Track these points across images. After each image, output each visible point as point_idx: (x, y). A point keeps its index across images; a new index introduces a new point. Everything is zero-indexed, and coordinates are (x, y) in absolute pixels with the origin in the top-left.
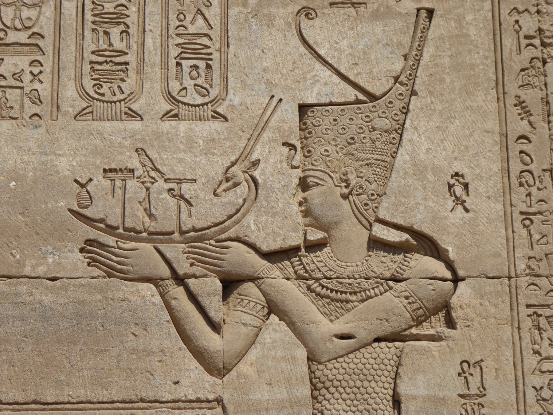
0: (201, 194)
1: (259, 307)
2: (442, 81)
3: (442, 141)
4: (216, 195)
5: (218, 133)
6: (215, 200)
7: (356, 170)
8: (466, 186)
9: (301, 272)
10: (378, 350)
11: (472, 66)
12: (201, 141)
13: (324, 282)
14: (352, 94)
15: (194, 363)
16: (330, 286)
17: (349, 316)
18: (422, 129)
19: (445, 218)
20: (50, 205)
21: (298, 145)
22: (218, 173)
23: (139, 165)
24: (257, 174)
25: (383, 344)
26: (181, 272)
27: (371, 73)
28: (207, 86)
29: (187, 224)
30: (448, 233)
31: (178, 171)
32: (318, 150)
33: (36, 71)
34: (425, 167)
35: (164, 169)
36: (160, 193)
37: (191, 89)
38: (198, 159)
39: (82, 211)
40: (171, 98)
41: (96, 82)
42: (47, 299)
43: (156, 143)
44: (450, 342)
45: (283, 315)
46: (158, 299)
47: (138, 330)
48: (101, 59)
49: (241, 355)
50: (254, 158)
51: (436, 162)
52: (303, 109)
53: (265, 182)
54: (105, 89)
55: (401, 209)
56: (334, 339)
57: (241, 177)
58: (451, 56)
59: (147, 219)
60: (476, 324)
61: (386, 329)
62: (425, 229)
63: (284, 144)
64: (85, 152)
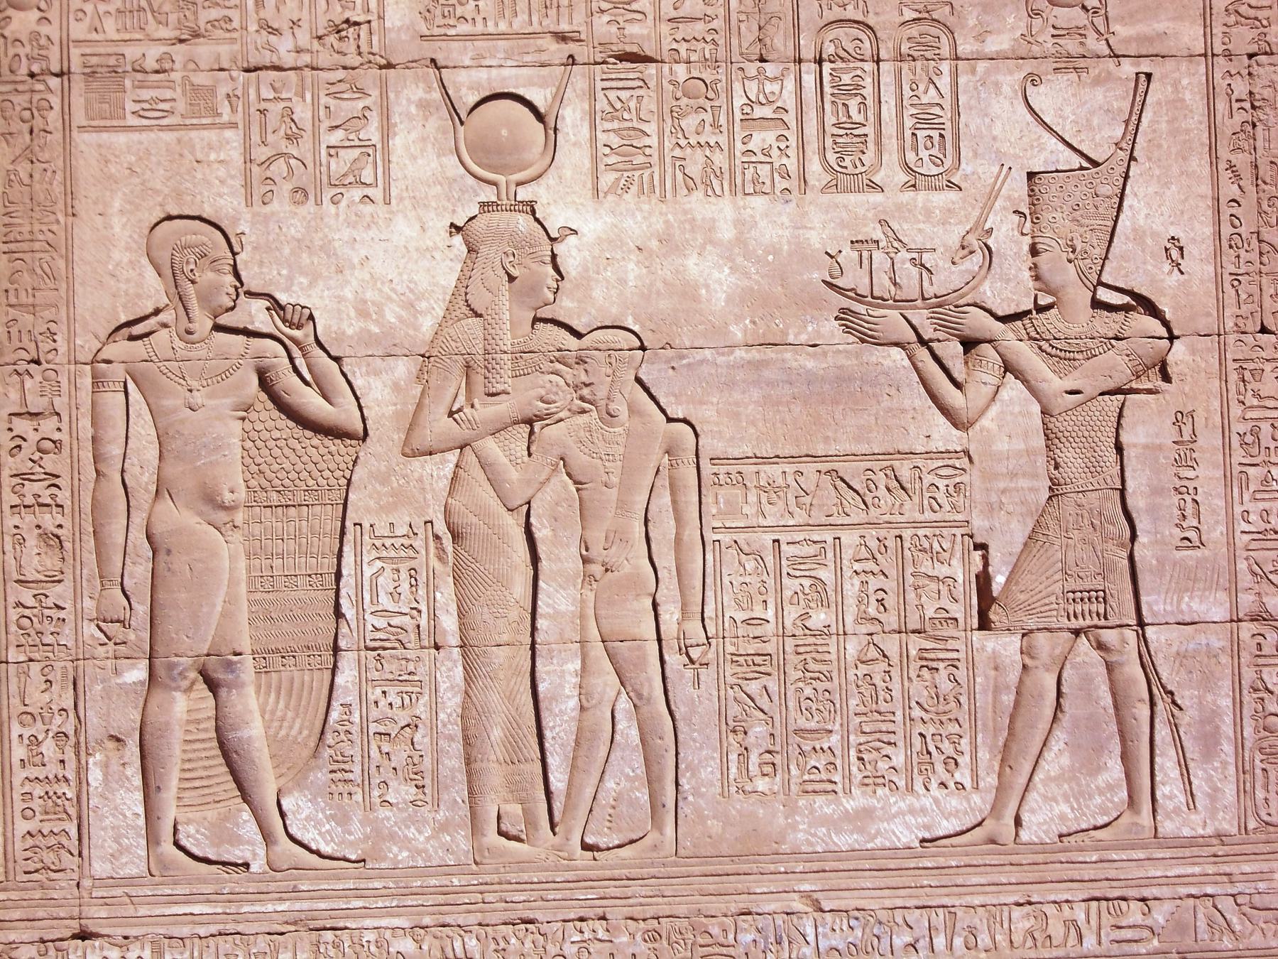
0: (941, 263)
1: (997, 367)
2: (1160, 146)
3: (1159, 207)
4: (953, 263)
5: (953, 203)
6: (953, 268)
7: (1081, 236)
8: (1181, 249)
9: (1033, 334)
10: (1102, 403)
11: (1188, 131)
12: (938, 212)
13: (1054, 342)
14: (1077, 161)
15: (942, 419)
16: (1059, 346)
17: (1076, 373)
18: (1141, 195)
19: (1163, 281)
20: (805, 277)
21: (1027, 212)
22: (954, 241)
23: (882, 237)
24: (990, 242)
25: (1107, 397)
26: (926, 338)
27: (1093, 140)
28: (941, 156)
29: (929, 291)
30: (1165, 296)
31: (919, 241)
32: (1046, 216)
33: (783, 146)
34: (1144, 232)
35: (905, 240)
36: (903, 263)
37: (926, 159)
38: (935, 230)
39: (834, 281)
40: (907, 168)
41: (839, 155)
42: (810, 364)
43: (897, 214)
44: (1167, 397)
45: (1019, 375)
46: (907, 362)
47: (893, 392)
48: (842, 132)
49: (983, 412)
50: (987, 227)
51: (1154, 226)
52: (1031, 175)
53: (998, 250)
54: (847, 163)
55: (1123, 272)
56: (1064, 395)
57: (976, 245)
58: (1168, 122)
59: (892, 288)
60: (1188, 378)
61: (1111, 385)
62: (1144, 291)
63: (1014, 212)
64: (833, 225)
